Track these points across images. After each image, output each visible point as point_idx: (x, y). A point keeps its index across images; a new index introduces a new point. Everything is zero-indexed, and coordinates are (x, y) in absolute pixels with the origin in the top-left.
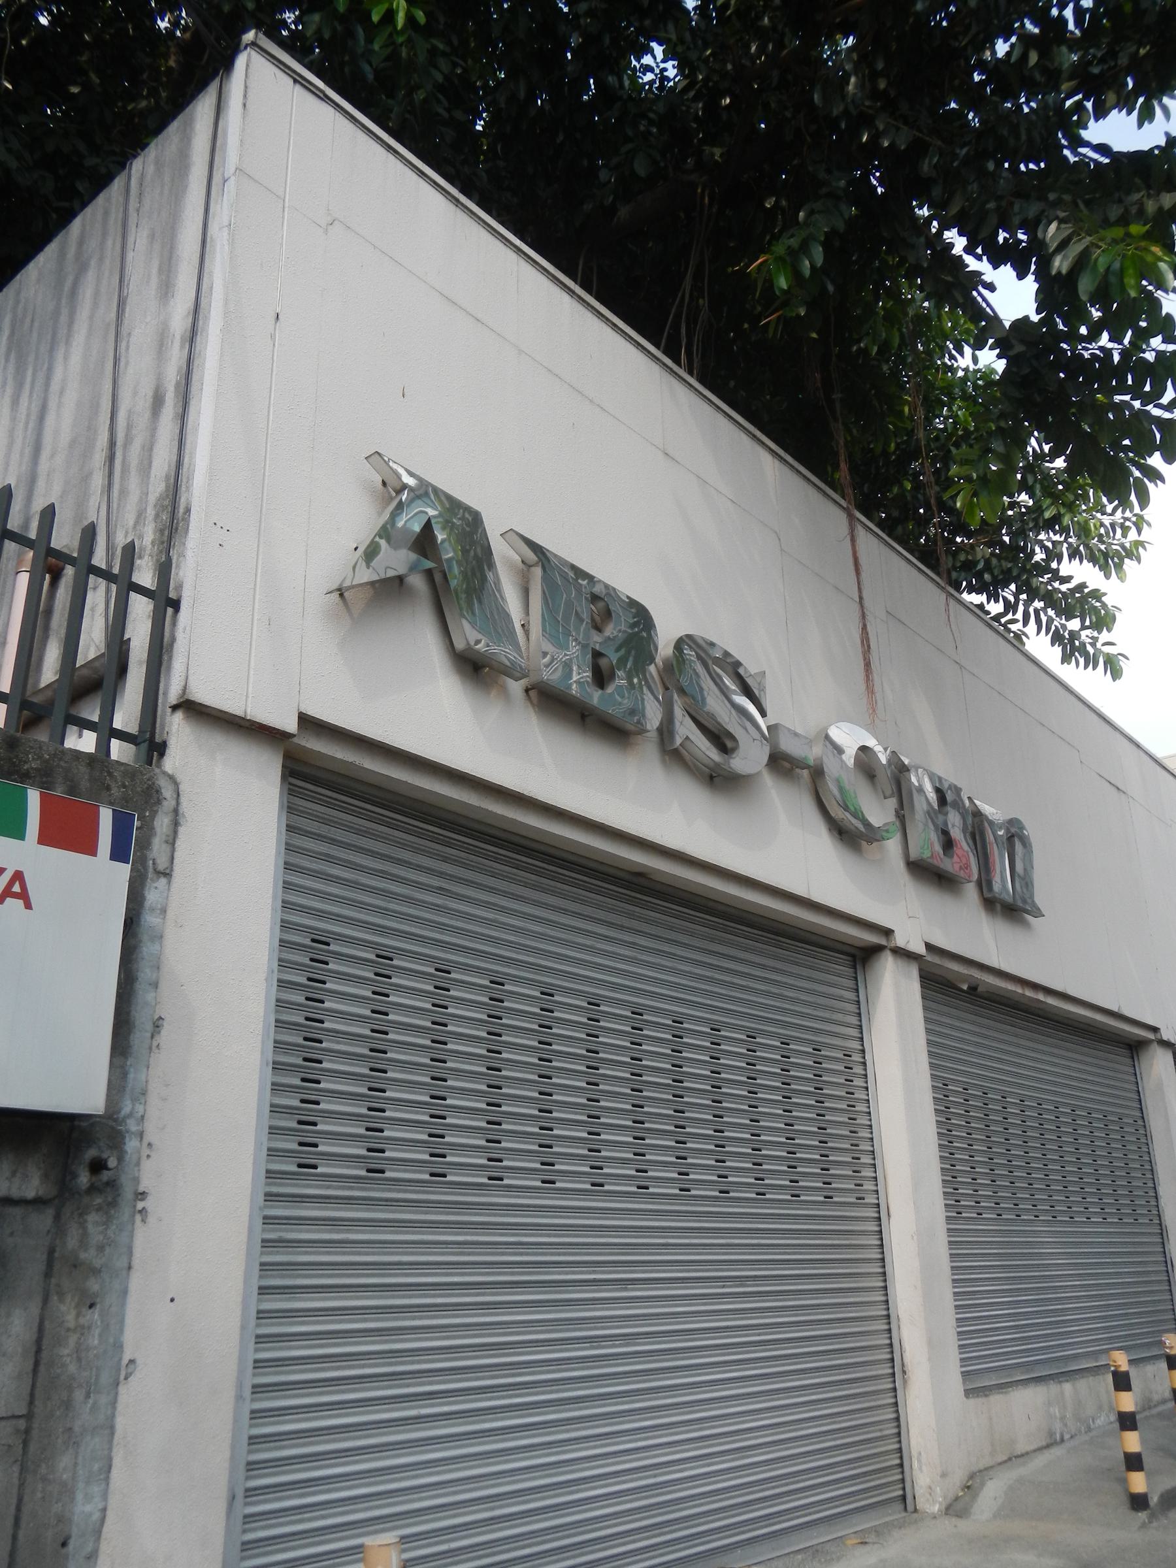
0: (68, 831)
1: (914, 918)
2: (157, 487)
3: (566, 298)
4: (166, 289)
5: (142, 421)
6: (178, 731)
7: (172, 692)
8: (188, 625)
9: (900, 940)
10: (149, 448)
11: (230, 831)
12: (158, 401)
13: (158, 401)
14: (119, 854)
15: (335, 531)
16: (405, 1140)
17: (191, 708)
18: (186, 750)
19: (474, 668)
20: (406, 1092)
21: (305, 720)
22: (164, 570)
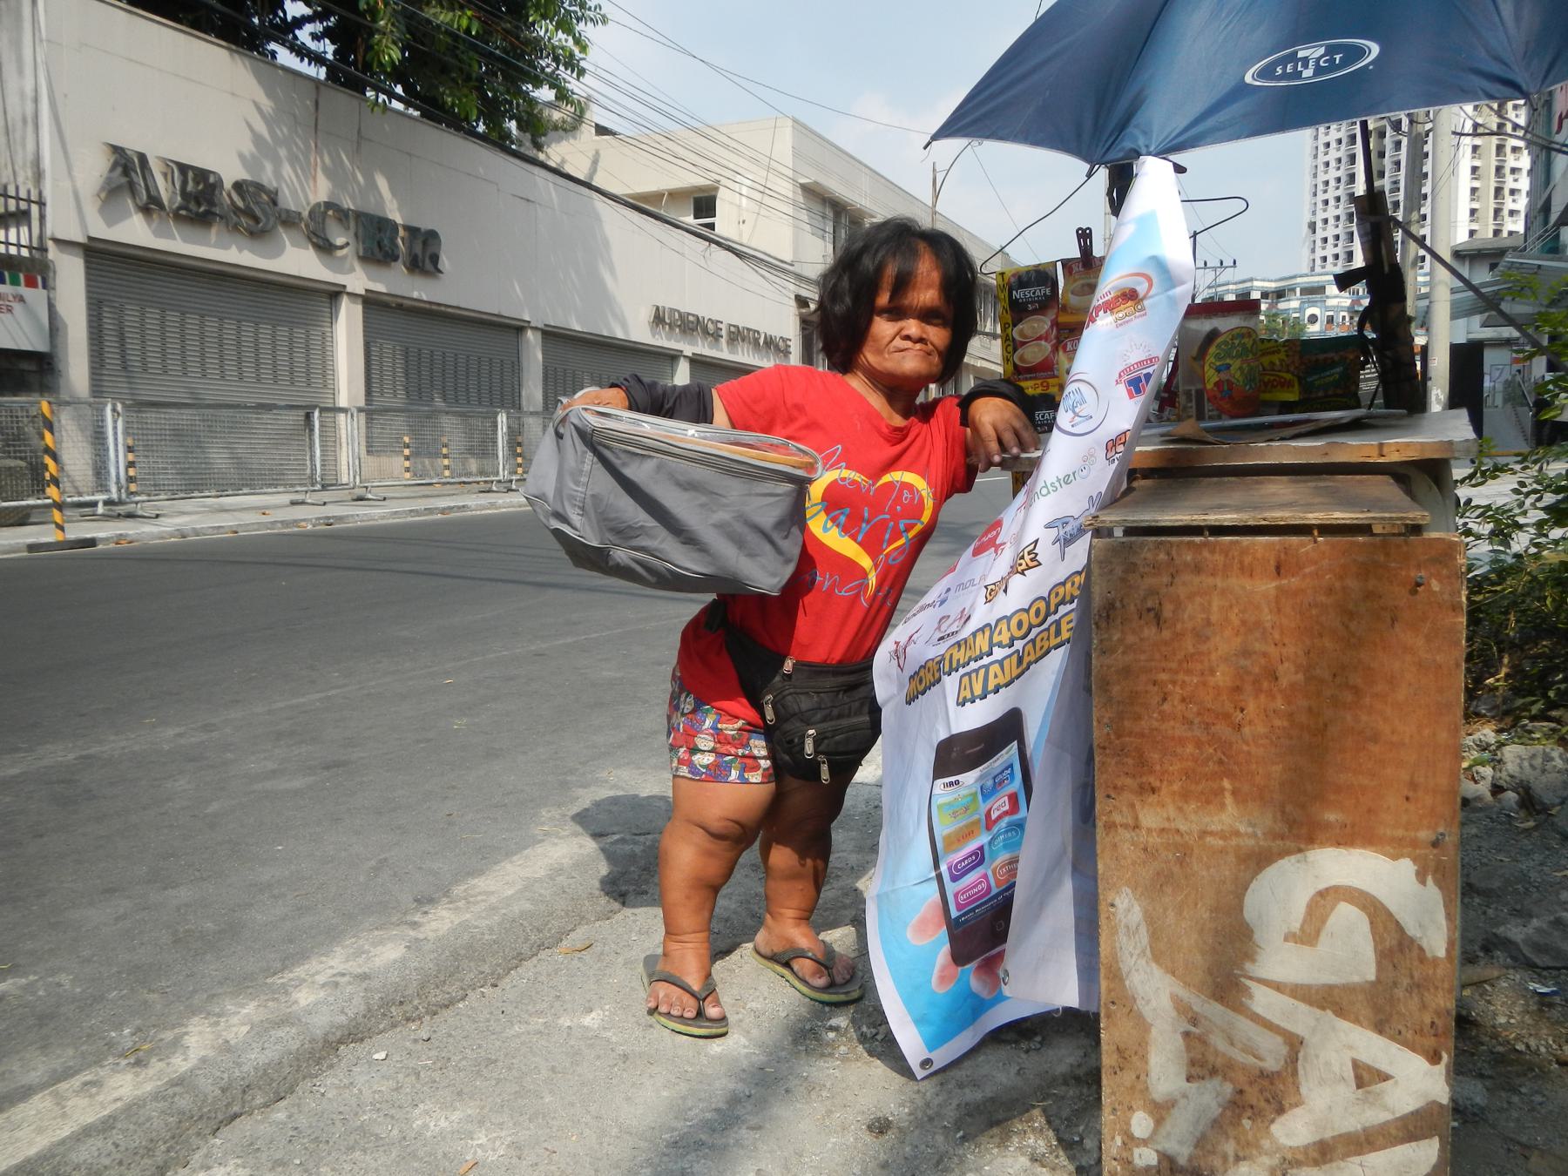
0: (31, 283)
1: (358, 280)
2: (30, 157)
3: (182, 36)
4: (20, 71)
5: (19, 124)
6: (50, 244)
7: (49, 233)
8: (49, 210)
9: (349, 289)
10: (24, 138)
11: (71, 274)
12: (24, 121)
13: (24, 121)
14: (45, 287)
15: (93, 168)
16: (134, 359)
17: (57, 241)
18: (53, 253)
19: (145, 210)
20: (133, 345)
21: (90, 238)
22: (40, 194)
